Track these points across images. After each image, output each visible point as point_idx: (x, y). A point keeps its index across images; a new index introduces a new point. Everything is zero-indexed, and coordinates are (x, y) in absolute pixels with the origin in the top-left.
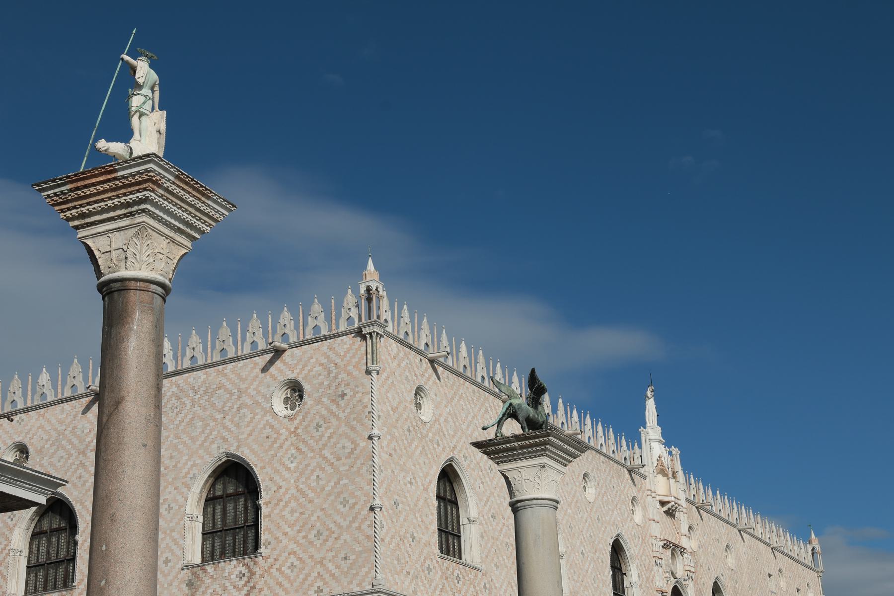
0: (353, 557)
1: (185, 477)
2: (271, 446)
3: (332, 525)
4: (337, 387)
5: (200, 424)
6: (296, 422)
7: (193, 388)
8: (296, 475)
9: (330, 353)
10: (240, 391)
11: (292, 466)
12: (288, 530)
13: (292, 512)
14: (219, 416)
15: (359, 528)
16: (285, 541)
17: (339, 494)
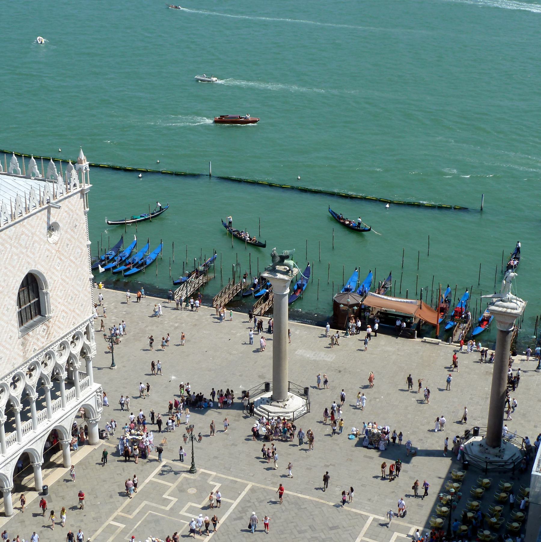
0: (85, 303)
1: (13, 289)
2: (49, 261)
3: (76, 292)
4: (73, 223)
5: (16, 257)
6: (58, 245)
7: (9, 237)
8: (61, 272)
9: (69, 205)
10: (32, 234)
11: (58, 268)
12: (60, 300)
13: (61, 291)
14: (24, 251)
15: (86, 290)
16: (59, 306)
17: (78, 276)
